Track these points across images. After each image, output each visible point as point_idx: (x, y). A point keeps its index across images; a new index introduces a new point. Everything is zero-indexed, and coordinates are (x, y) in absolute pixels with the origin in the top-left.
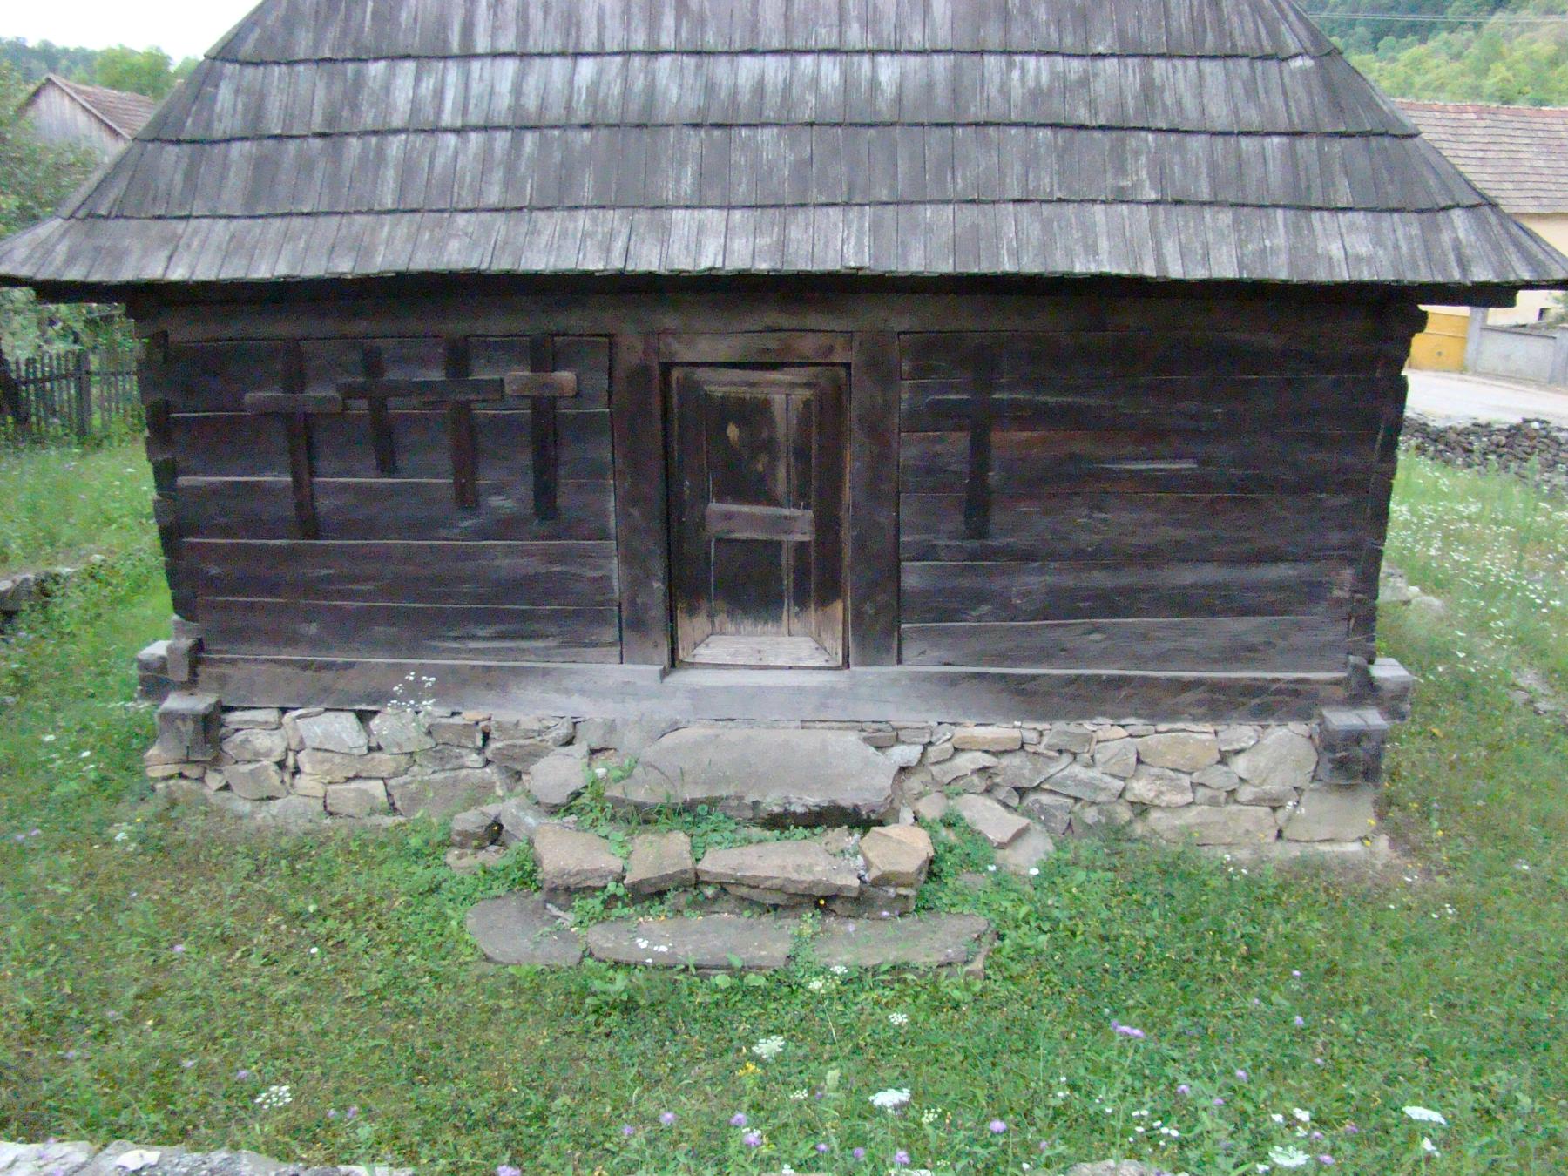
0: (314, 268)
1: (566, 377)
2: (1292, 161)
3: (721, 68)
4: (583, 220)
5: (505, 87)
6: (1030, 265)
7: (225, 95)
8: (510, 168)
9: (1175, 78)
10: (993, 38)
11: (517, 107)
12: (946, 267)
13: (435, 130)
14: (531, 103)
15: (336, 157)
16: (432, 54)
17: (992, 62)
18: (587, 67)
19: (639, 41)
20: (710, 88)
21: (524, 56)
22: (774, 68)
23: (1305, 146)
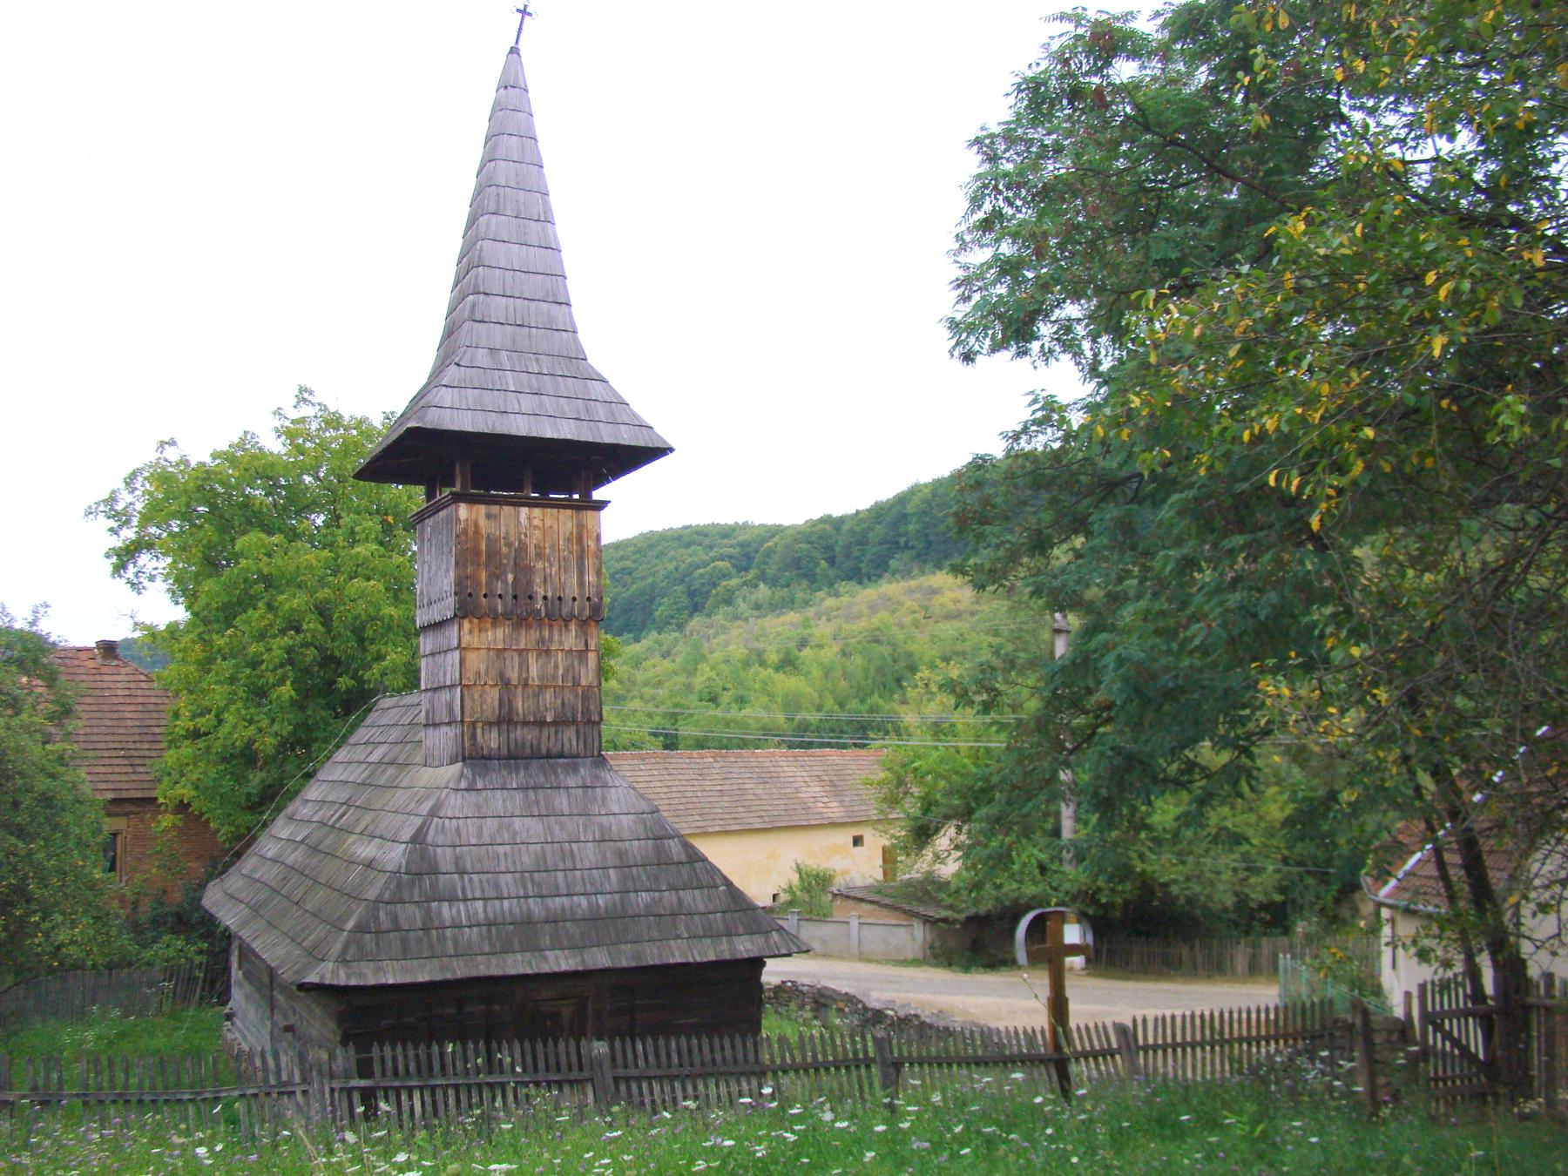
0: (439, 977)
1: (497, 1008)
2: (724, 920)
3: (549, 901)
4: (519, 956)
5: (481, 910)
6: (657, 962)
7: (382, 915)
8: (490, 938)
9: (686, 896)
10: (630, 886)
11: (487, 917)
12: (633, 964)
13: (461, 926)
14: (491, 916)
15: (429, 937)
16: (452, 899)
17: (632, 895)
18: (506, 903)
19: (521, 893)
20: (547, 909)
21: (485, 899)
22: (565, 899)
23: (728, 915)
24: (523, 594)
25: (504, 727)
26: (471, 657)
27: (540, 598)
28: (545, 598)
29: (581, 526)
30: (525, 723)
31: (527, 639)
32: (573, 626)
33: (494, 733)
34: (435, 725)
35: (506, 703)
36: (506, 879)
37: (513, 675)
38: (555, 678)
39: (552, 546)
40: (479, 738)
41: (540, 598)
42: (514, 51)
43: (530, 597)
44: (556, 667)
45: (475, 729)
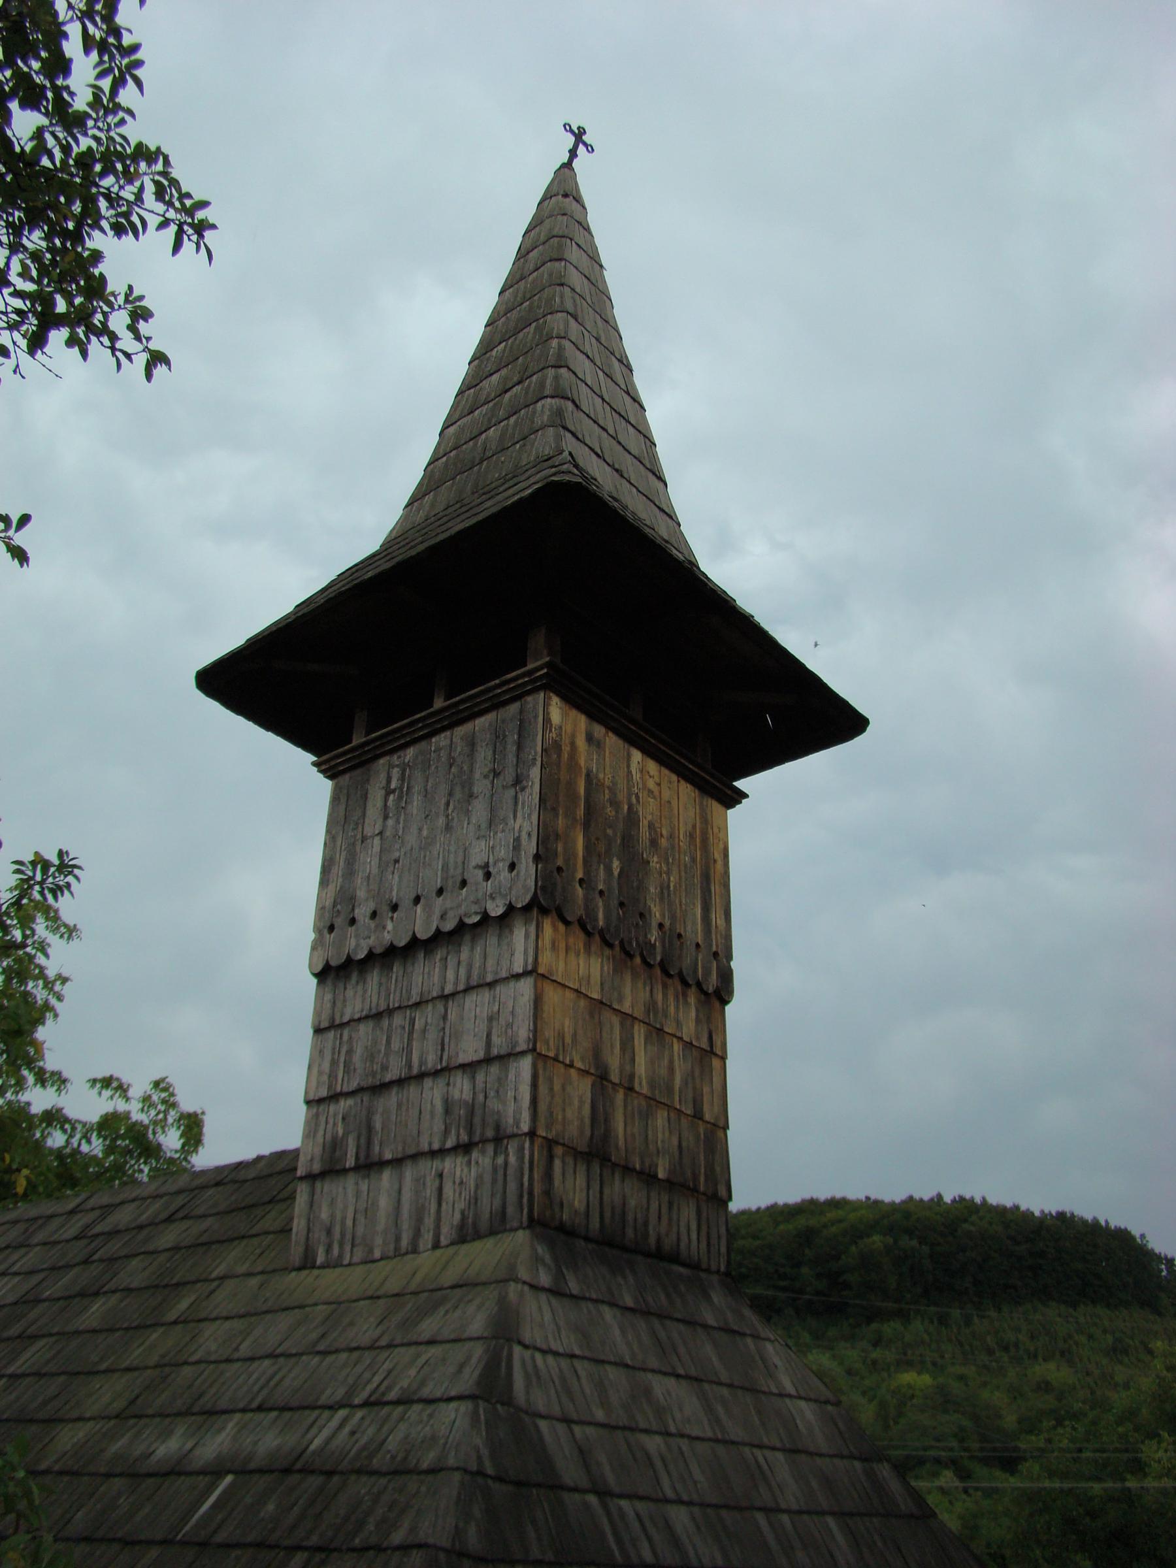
24: (630, 903)
25: (596, 1168)
26: (552, 996)
27: (654, 924)
28: (661, 926)
29: (705, 821)
30: (627, 1170)
31: (633, 995)
32: (692, 1000)
33: (581, 1180)
34: (369, 1166)
35: (599, 1117)
36: (680, 1517)
37: (614, 1061)
38: (670, 1090)
39: (671, 836)
40: (557, 1181)
41: (654, 924)
42: (568, 165)
43: (642, 915)
44: (671, 1069)
45: (551, 1158)
